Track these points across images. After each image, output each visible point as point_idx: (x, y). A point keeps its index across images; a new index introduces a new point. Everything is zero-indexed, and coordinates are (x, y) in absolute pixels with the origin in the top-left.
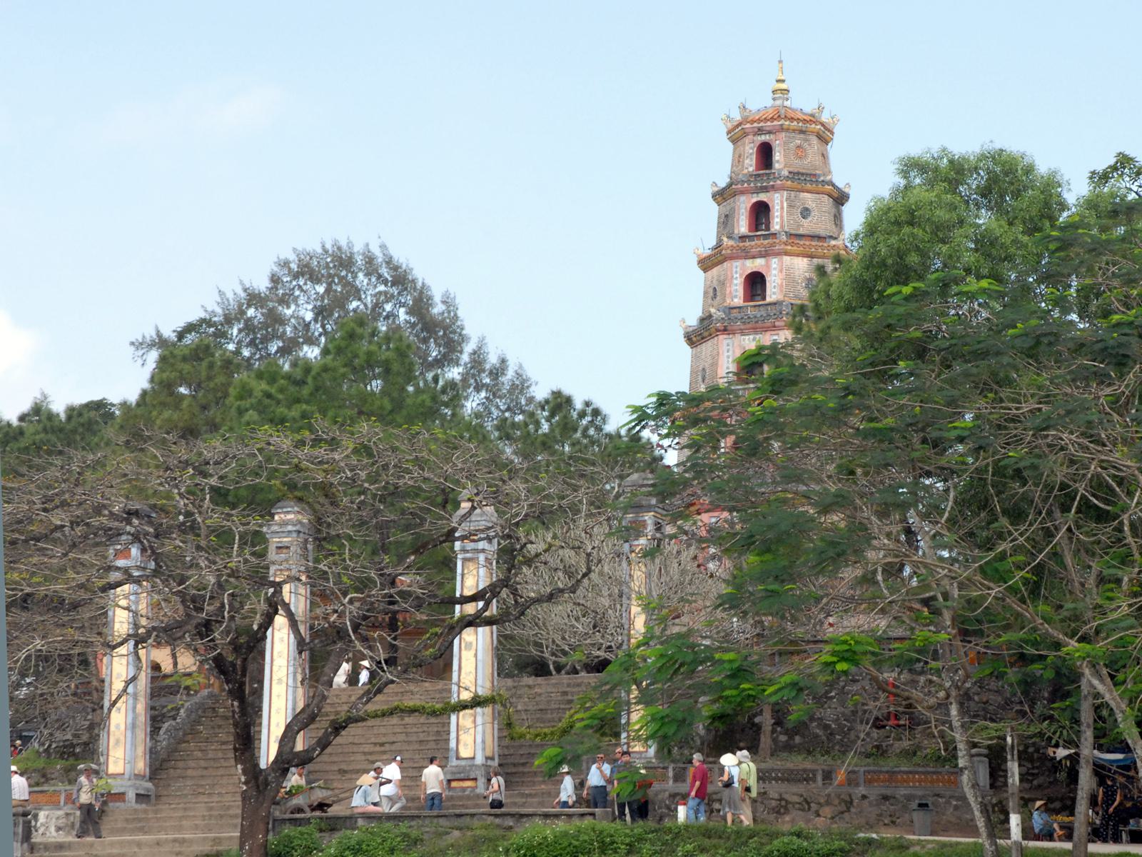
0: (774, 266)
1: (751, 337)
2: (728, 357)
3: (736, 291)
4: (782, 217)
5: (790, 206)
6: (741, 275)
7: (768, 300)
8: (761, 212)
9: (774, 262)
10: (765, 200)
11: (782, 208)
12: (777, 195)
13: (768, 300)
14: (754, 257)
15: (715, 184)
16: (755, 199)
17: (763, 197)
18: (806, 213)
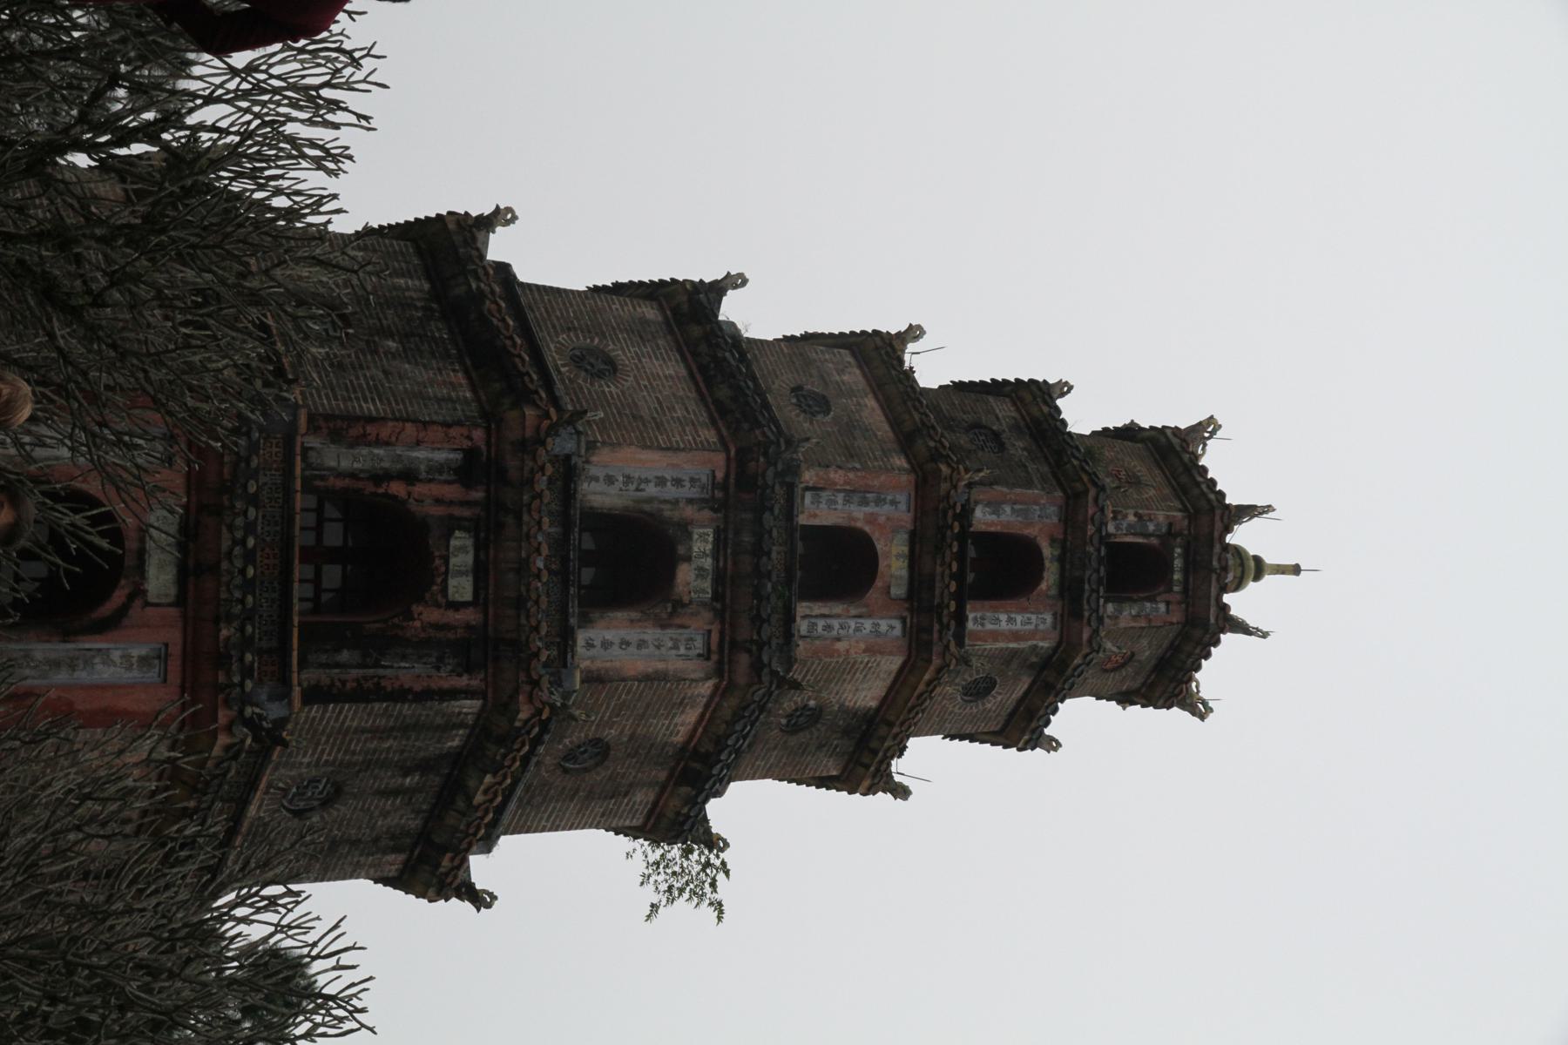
0: (884, 625)
1: (708, 563)
2: (661, 481)
3: (832, 502)
4: (995, 635)
5: (1014, 653)
6: (871, 519)
7: (802, 608)
8: (1005, 568)
9: (891, 627)
10: (1043, 586)
11: (1016, 636)
12: (1049, 618)
13: (802, 608)
14: (913, 560)
15: (1064, 388)
16: (1047, 551)
17: (1050, 578)
18: (979, 690)
